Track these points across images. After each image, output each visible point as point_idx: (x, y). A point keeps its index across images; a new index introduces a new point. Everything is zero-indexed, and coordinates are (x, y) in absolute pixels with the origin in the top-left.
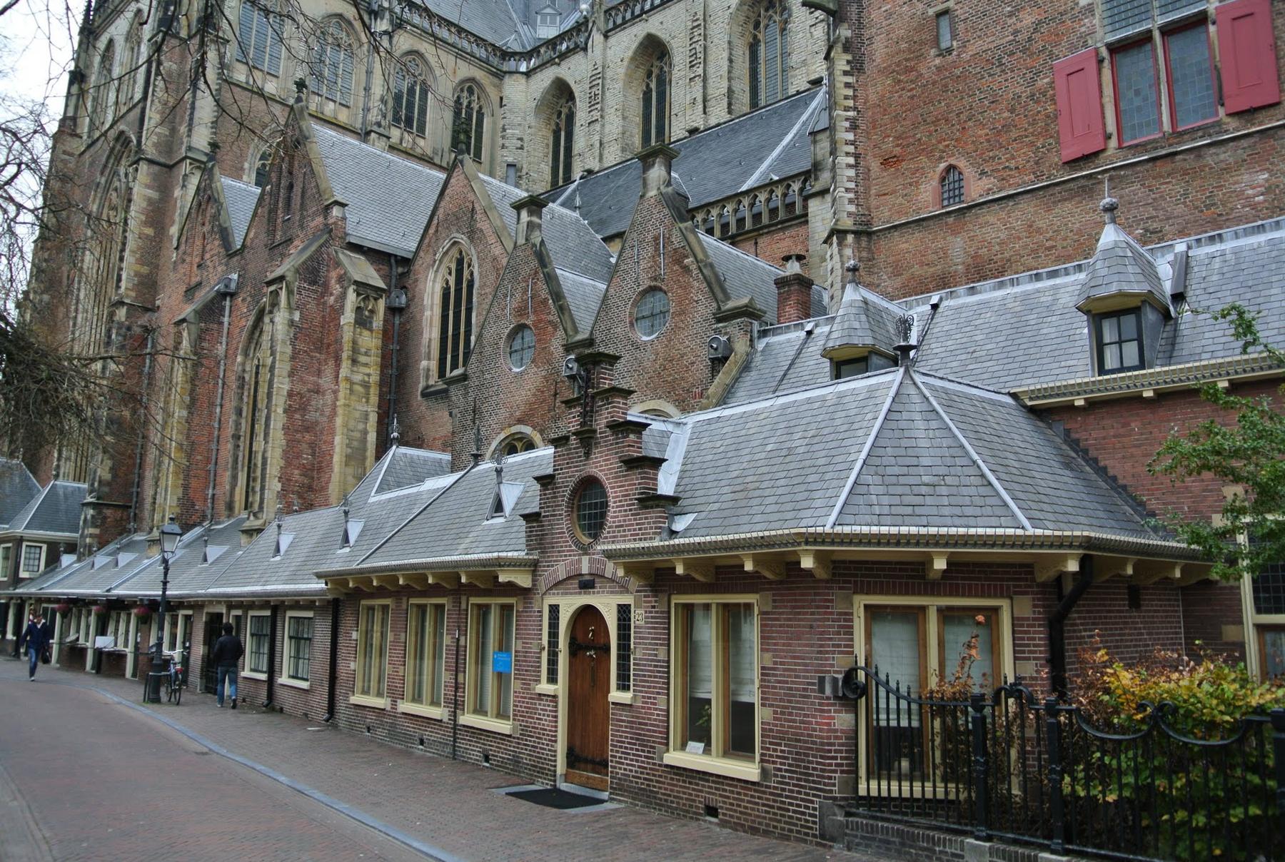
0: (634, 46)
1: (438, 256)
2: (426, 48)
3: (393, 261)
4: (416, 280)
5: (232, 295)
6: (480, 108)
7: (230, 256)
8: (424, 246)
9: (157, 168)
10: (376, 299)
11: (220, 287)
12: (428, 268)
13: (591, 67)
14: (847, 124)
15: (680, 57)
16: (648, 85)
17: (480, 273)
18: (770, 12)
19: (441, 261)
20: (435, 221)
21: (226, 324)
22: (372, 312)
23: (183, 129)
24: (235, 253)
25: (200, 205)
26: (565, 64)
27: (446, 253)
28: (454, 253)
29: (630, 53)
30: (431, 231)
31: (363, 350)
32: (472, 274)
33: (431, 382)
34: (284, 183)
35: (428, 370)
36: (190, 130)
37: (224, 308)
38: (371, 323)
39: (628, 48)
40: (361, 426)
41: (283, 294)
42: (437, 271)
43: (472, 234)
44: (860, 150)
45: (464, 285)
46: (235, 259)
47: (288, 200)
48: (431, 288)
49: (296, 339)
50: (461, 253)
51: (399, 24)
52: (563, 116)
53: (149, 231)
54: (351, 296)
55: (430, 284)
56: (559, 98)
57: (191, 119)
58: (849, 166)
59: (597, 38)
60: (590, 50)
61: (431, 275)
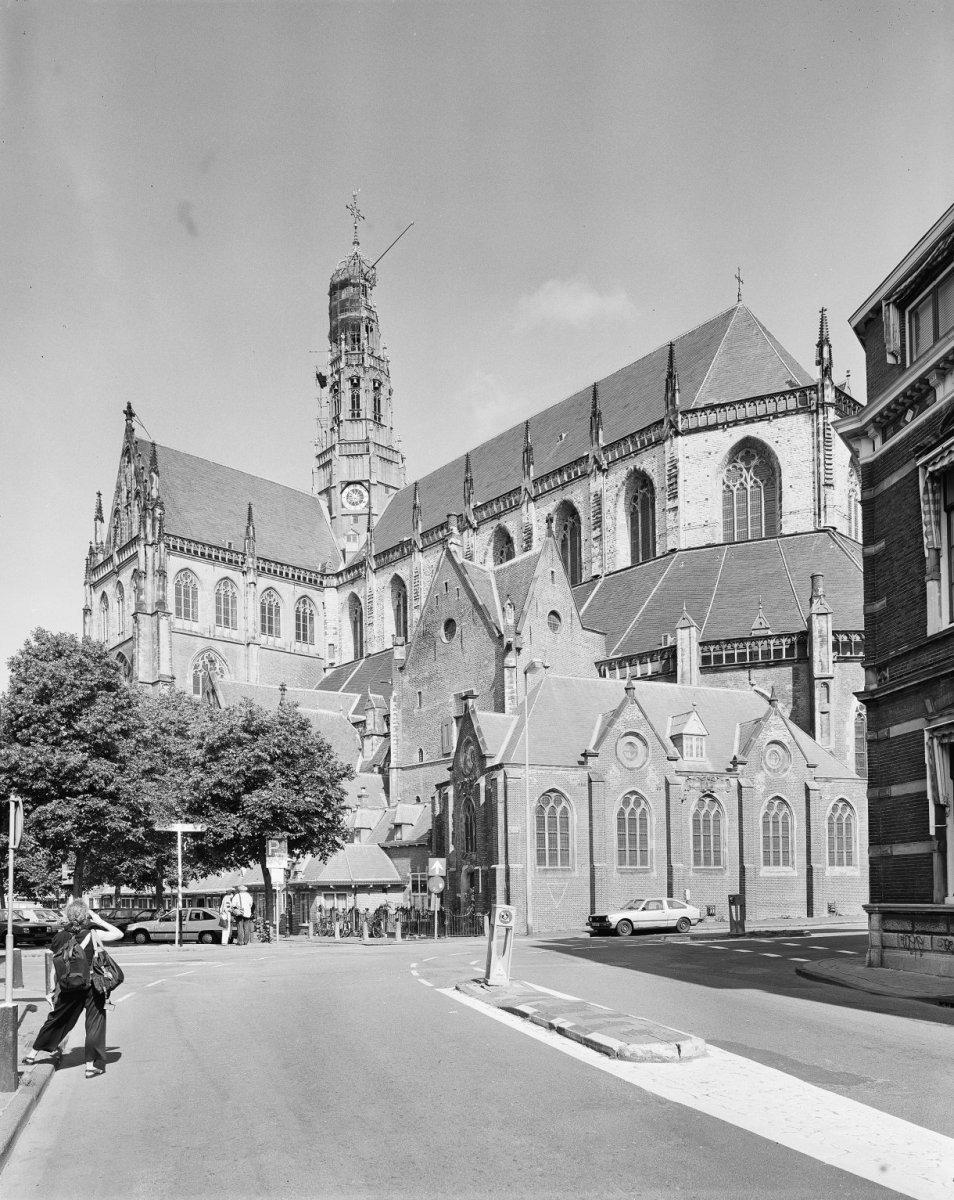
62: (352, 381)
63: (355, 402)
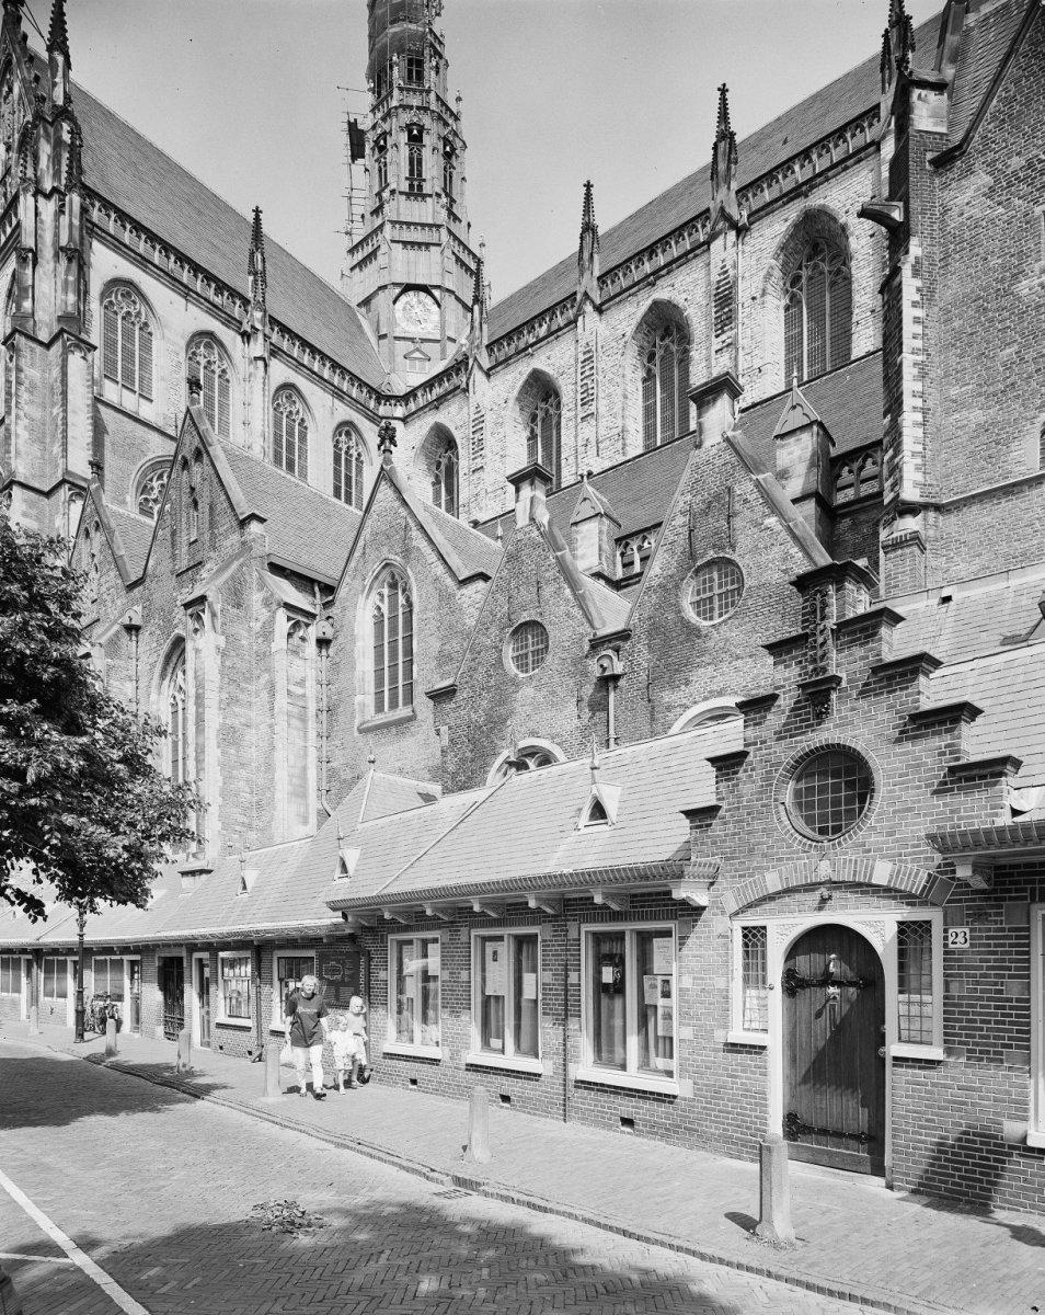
0: (520, 383)
1: (368, 582)
6: (359, 455)
10: (307, 625)
15: (568, 393)
16: (532, 431)
18: (667, 341)
20: (361, 543)
29: (515, 393)
39: (513, 388)
44: (930, 404)
50: (393, 577)
52: (443, 467)
56: (438, 447)
58: (916, 424)
59: (478, 376)
60: (471, 389)
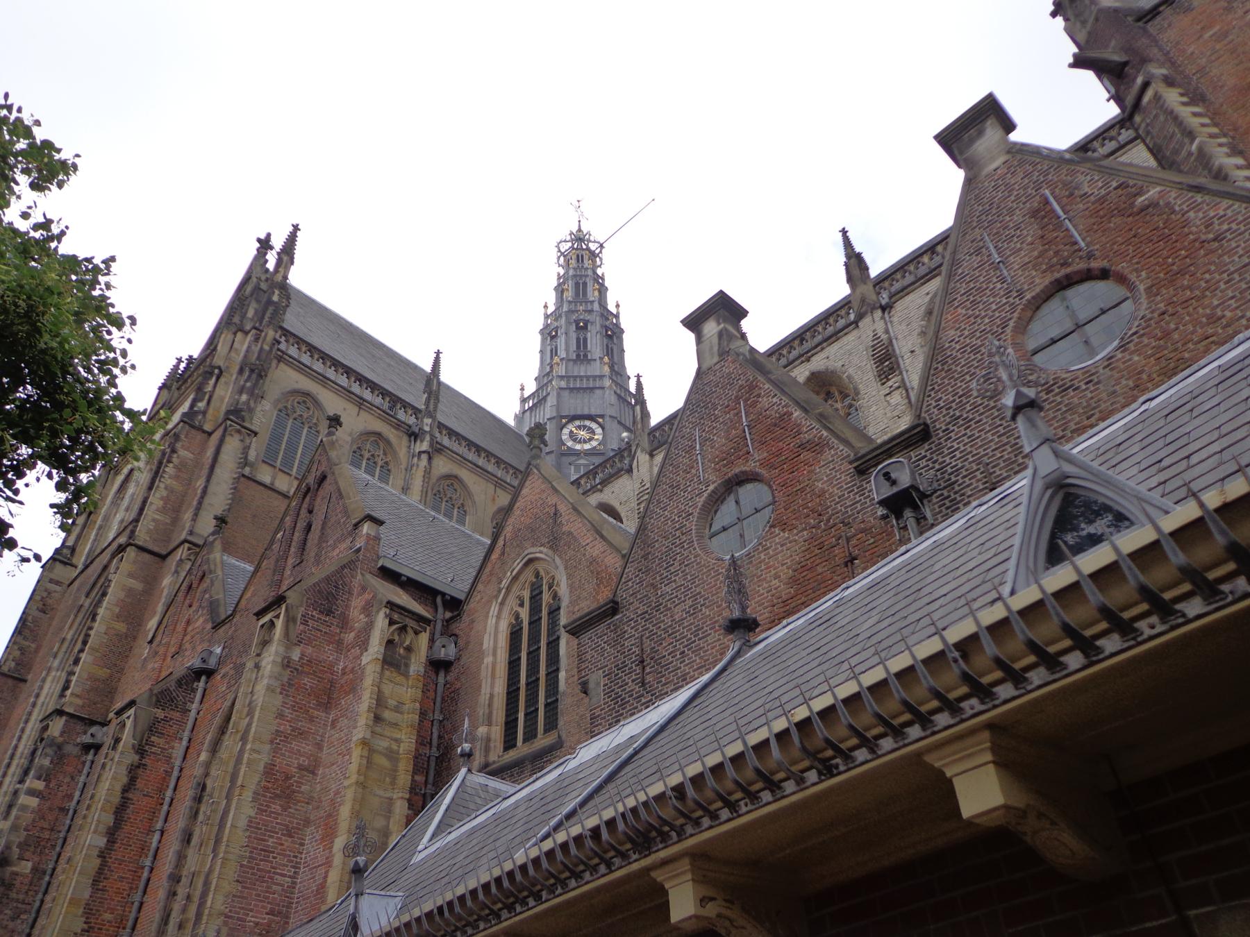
1: (505, 583)
2: (464, 474)
3: (439, 599)
4: (473, 621)
5: (210, 673)
7: (216, 627)
8: (484, 577)
9: (147, 556)
10: (416, 633)
11: (196, 663)
12: (489, 602)
13: (637, 485)
14: (1225, 149)
17: (571, 587)
19: (508, 590)
21: (193, 714)
22: (409, 649)
23: (188, 516)
24: (223, 622)
25: (190, 587)
26: (607, 490)
27: (515, 578)
28: (529, 576)
30: (494, 556)
31: (392, 703)
32: (555, 596)
33: (493, 757)
34: (301, 525)
35: (488, 740)
36: (196, 515)
37: (194, 691)
38: (407, 666)
40: (379, 823)
41: (279, 624)
42: (502, 604)
43: (555, 542)
45: (544, 613)
46: (221, 631)
47: (305, 541)
48: (492, 630)
49: (290, 685)
50: (537, 575)
51: (437, 449)
53: (121, 627)
54: (381, 621)
55: (491, 621)
57: (200, 503)
61: (494, 609)
62: (577, 325)
63: (582, 344)
